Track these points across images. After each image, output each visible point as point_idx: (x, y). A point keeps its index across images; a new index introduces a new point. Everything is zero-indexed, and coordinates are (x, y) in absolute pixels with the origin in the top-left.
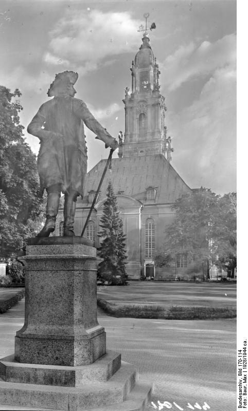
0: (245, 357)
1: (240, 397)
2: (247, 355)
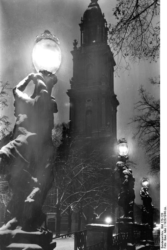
0: (165, 217)
1: (162, 241)
2: (166, 216)
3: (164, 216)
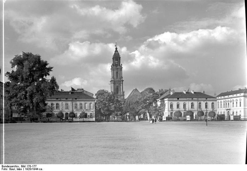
1: (9, 166)
3: (33, 168)
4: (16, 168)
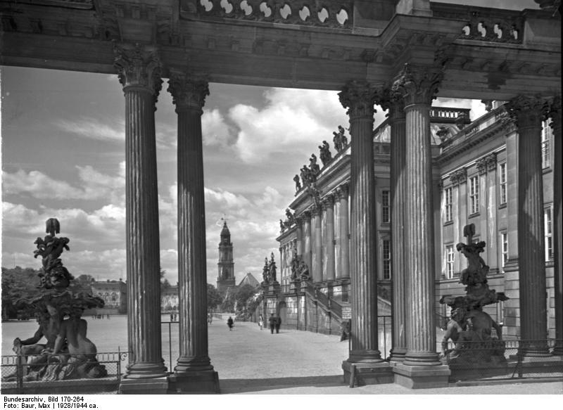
1: (20, 400)
4: (36, 404)
